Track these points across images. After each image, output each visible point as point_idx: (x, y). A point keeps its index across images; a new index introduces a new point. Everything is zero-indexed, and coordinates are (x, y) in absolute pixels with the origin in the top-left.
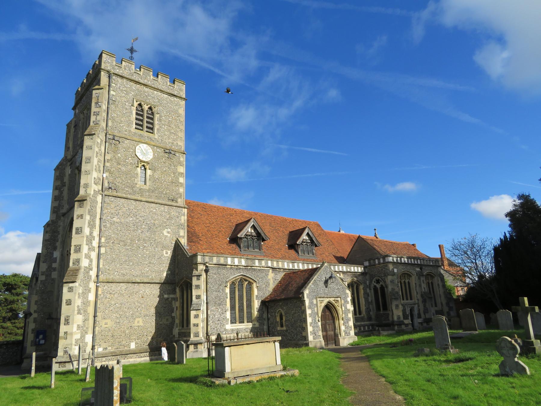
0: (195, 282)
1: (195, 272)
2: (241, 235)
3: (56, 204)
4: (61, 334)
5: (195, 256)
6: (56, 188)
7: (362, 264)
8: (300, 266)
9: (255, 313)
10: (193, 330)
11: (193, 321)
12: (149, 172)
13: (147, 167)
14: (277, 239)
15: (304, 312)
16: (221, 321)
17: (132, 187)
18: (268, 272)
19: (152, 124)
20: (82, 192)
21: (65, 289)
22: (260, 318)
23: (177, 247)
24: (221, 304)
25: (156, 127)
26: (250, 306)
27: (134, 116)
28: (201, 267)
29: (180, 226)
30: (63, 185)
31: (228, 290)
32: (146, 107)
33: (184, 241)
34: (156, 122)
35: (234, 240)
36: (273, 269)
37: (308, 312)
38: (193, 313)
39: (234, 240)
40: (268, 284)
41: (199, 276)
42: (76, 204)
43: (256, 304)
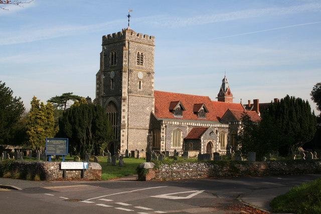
0: (162, 131)
1: (162, 127)
2: (175, 109)
3: (98, 91)
4: (121, 145)
5: (162, 121)
6: (97, 84)
7: (228, 123)
8: (199, 125)
9: (182, 144)
10: (161, 147)
11: (162, 144)
12: (142, 83)
13: (141, 81)
14: (189, 109)
15: (201, 144)
16: (170, 145)
17: (136, 91)
18: (188, 125)
19: (142, 60)
20: (123, 95)
21: (121, 131)
22: (183, 145)
23: (152, 115)
24: (170, 139)
25: (144, 62)
26: (179, 141)
27: (137, 58)
28: (164, 125)
29: (152, 106)
30: (101, 83)
31: (172, 134)
32: (140, 54)
33: (154, 112)
34: (144, 60)
35: (171, 111)
36: (189, 126)
37: (202, 144)
38: (162, 142)
39: (171, 111)
40: (186, 132)
41: (163, 129)
42: (122, 101)
43: (182, 140)
